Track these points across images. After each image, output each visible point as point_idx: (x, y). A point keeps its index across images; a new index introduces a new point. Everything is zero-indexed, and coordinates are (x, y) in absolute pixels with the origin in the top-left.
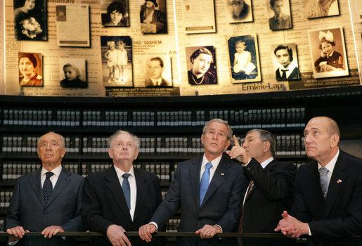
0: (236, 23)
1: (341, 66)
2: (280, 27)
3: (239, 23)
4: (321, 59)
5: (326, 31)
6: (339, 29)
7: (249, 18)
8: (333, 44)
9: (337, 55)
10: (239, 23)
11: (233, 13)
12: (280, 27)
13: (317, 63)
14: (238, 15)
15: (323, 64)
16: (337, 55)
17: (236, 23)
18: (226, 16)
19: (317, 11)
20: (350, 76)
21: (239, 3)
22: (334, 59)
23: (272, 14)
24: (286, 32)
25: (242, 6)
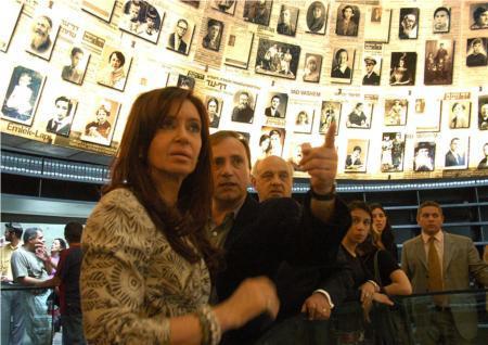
0: (31, 54)
1: (106, 136)
2: (71, 79)
3: (35, 55)
4: (93, 124)
5: (107, 100)
6: (117, 103)
7: (46, 54)
8: (108, 114)
9: (107, 125)
10: (35, 55)
11: (34, 41)
12: (71, 79)
13: (89, 126)
14: (37, 46)
15: (93, 129)
16: (107, 125)
17: (31, 54)
18: (27, 36)
19: (107, 81)
20: (109, 147)
21: (44, 34)
22: (103, 127)
23: (69, 63)
24: (74, 86)
25: (45, 39)
